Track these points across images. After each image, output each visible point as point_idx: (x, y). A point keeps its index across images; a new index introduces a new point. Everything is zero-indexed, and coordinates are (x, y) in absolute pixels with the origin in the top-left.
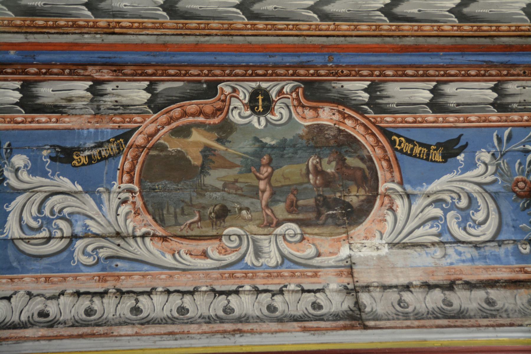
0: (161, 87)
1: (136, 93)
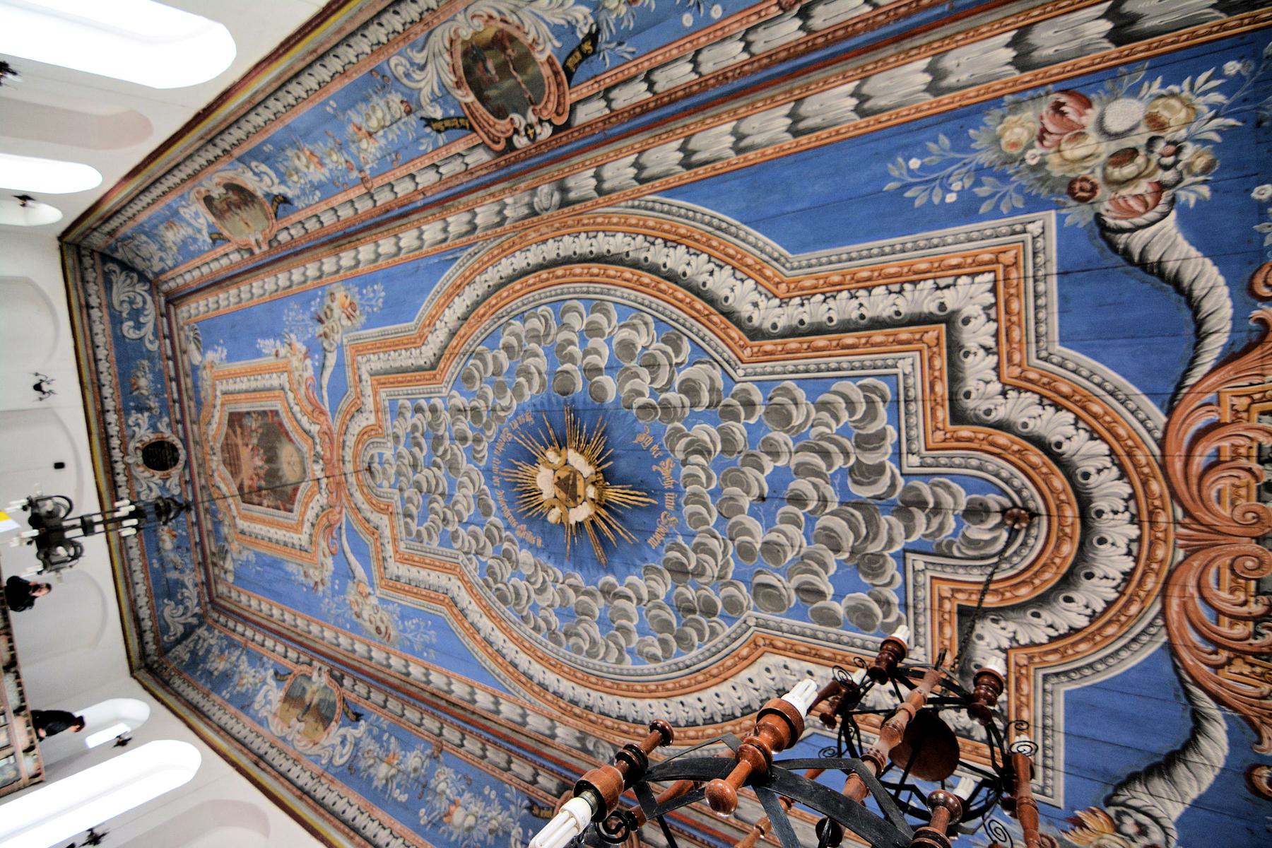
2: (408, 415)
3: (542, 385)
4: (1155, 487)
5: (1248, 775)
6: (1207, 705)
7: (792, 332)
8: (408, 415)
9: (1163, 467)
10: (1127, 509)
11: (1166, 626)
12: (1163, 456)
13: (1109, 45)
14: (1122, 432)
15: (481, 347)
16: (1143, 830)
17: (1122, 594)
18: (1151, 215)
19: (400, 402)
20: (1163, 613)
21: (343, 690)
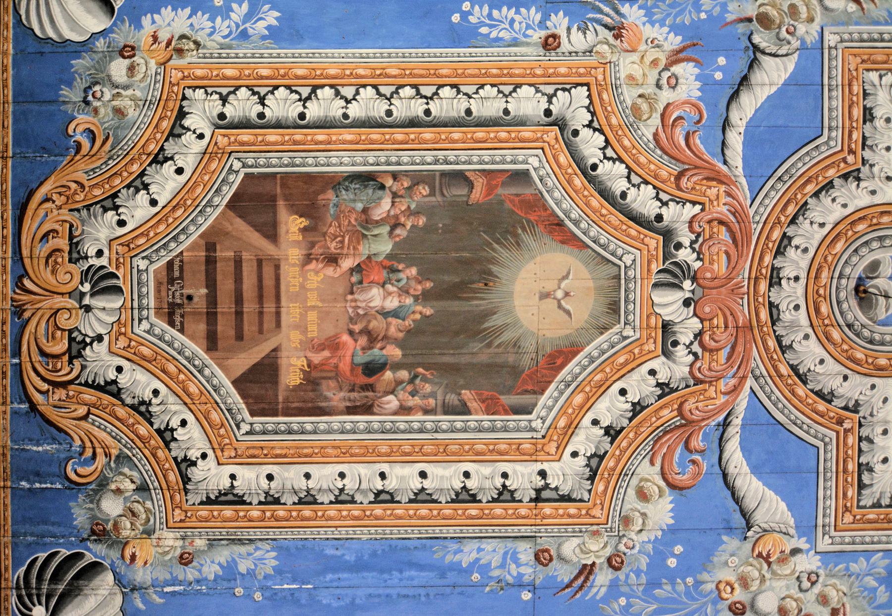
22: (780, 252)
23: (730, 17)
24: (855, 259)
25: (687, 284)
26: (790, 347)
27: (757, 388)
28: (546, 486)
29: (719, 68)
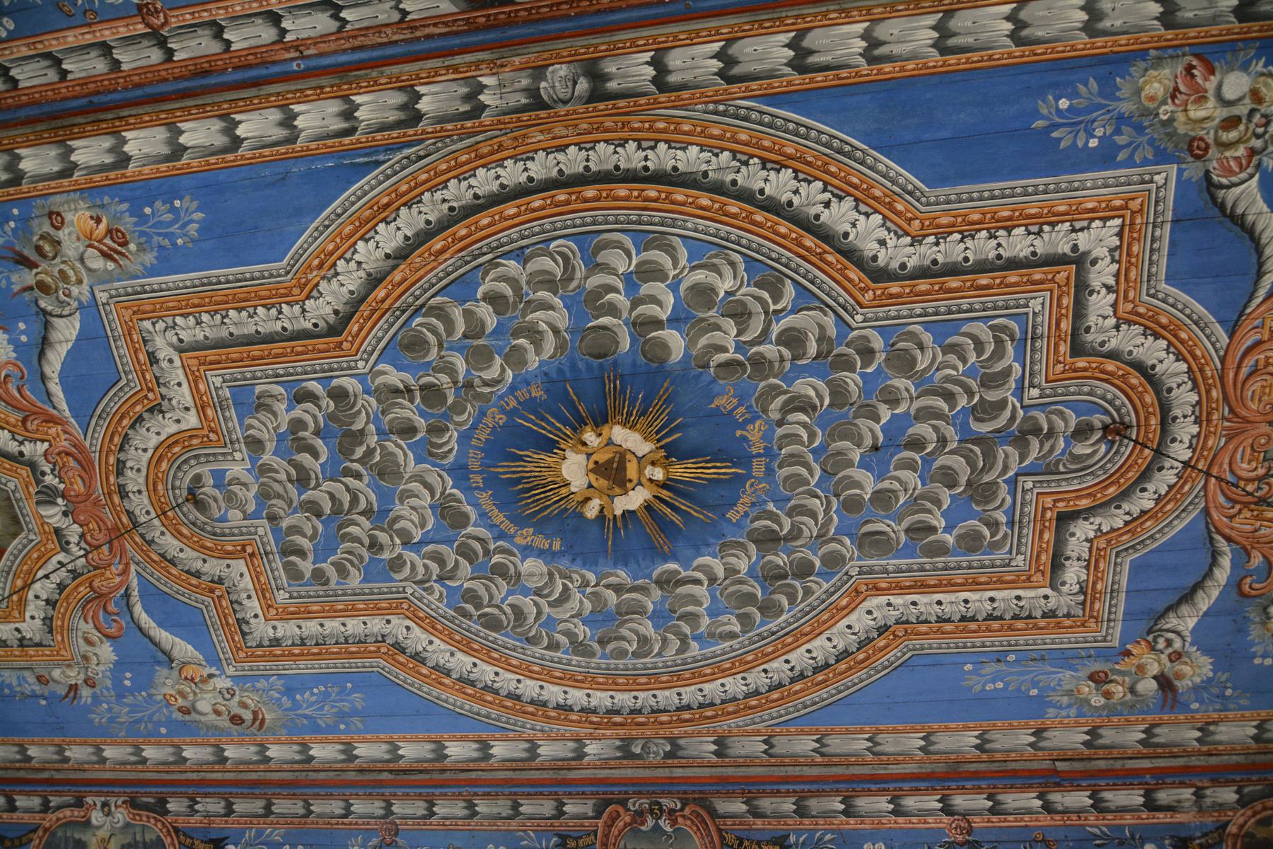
0: (1246, 790)
1: (1228, 795)
2: (281, 407)
3: (561, 346)
4: (1214, 393)
5: (1239, 585)
6: (1222, 544)
7: (923, 273)
8: (281, 407)
9: (1222, 378)
10: (1193, 413)
11: (1206, 495)
12: (1223, 369)
13: (1234, 20)
14: (1198, 353)
15: (438, 299)
16: (1169, 643)
17: (1180, 478)
18: (1243, 176)
19: (258, 389)
20: (1205, 487)
21: (170, 818)
22: (120, 473)
23: (16, 288)
24: (180, 474)
25: (60, 501)
26: (153, 541)
27: (140, 570)
28: (23, 638)
29: (23, 332)
